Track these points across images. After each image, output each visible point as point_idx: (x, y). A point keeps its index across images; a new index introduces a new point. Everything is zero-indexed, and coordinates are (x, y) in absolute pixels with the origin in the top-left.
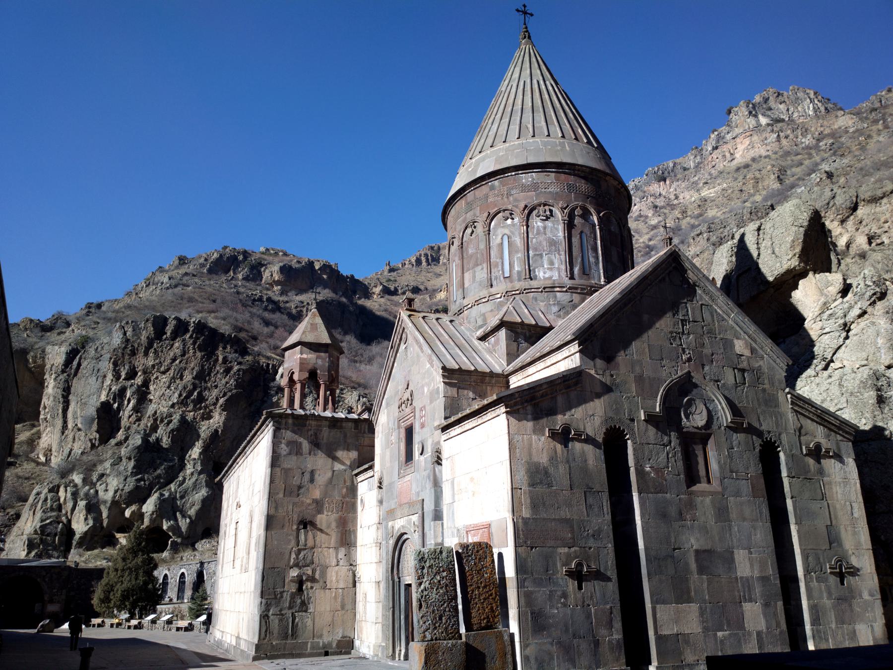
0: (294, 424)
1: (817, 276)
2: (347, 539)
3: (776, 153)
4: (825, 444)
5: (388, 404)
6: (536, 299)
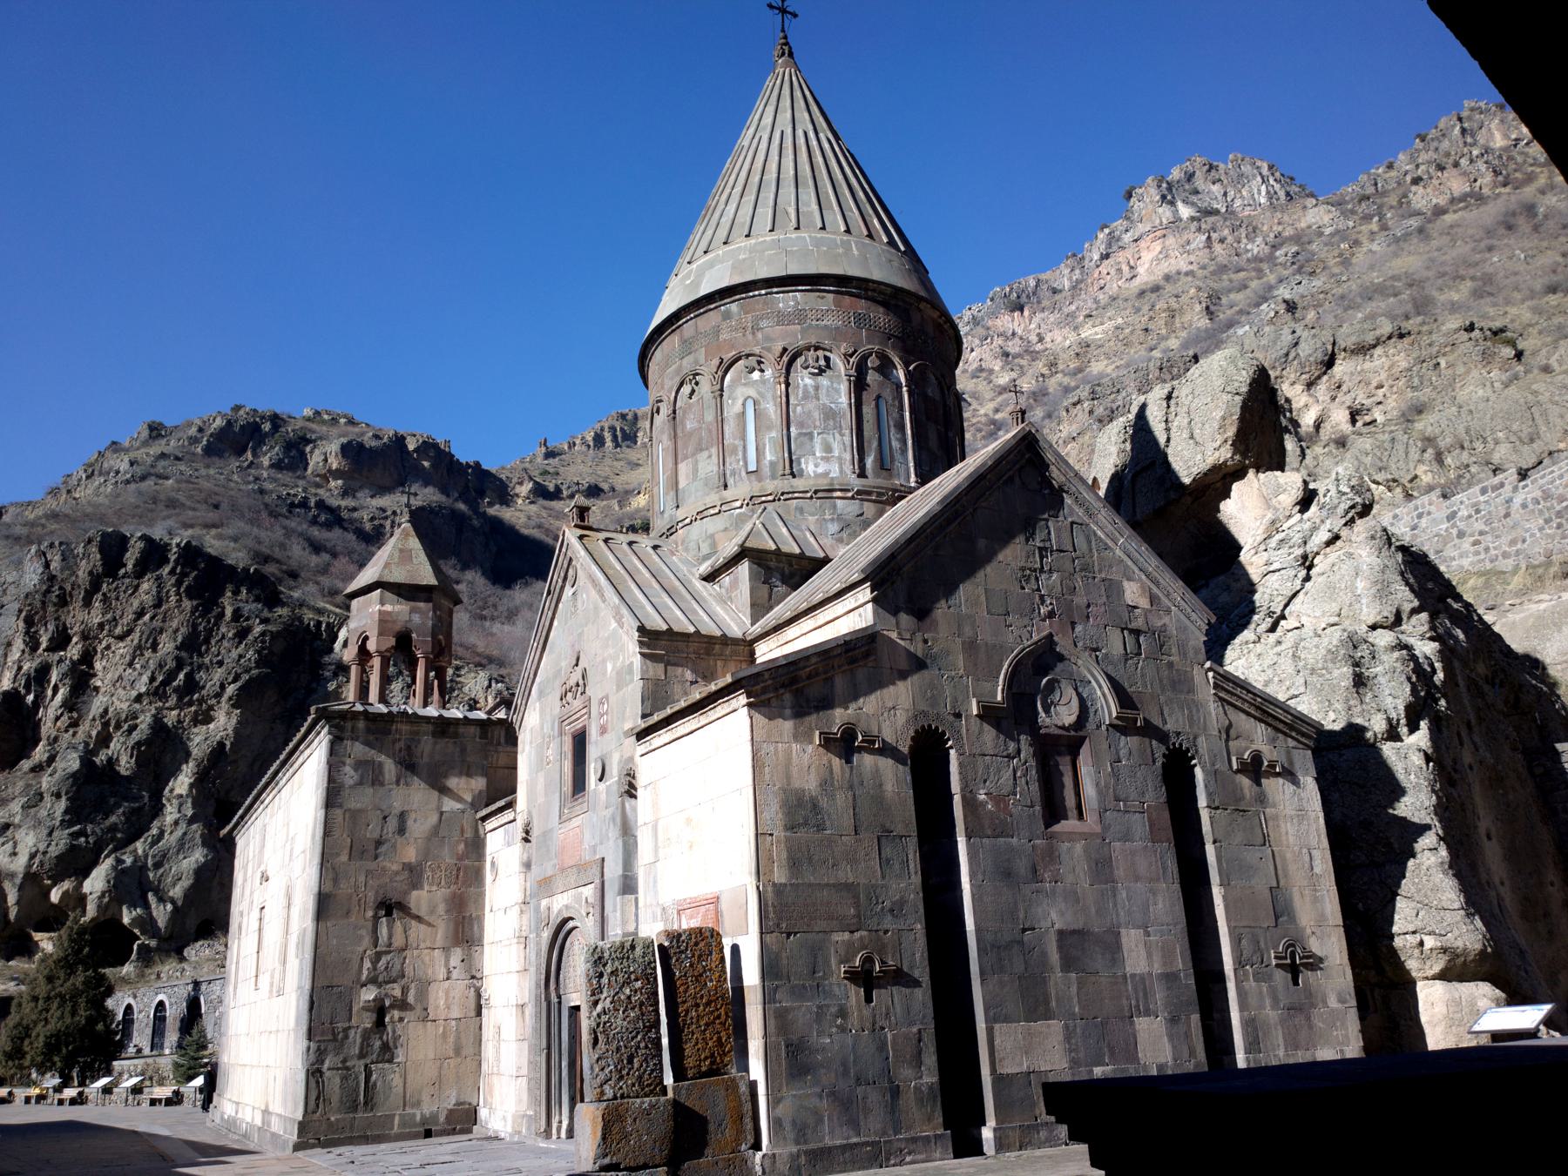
0: (368, 730)
1: (1261, 476)
2: (465, 931)
3: (1204, 267)
4: (1268, 754)
5: (541, 694)
6: (801, 510)
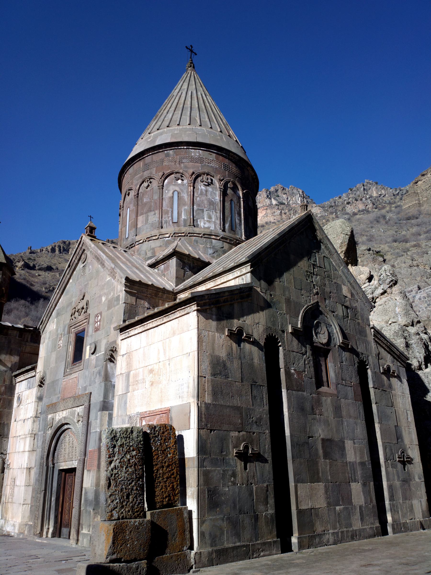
5: (58, 315)
6: (197, 242)
